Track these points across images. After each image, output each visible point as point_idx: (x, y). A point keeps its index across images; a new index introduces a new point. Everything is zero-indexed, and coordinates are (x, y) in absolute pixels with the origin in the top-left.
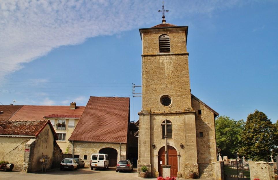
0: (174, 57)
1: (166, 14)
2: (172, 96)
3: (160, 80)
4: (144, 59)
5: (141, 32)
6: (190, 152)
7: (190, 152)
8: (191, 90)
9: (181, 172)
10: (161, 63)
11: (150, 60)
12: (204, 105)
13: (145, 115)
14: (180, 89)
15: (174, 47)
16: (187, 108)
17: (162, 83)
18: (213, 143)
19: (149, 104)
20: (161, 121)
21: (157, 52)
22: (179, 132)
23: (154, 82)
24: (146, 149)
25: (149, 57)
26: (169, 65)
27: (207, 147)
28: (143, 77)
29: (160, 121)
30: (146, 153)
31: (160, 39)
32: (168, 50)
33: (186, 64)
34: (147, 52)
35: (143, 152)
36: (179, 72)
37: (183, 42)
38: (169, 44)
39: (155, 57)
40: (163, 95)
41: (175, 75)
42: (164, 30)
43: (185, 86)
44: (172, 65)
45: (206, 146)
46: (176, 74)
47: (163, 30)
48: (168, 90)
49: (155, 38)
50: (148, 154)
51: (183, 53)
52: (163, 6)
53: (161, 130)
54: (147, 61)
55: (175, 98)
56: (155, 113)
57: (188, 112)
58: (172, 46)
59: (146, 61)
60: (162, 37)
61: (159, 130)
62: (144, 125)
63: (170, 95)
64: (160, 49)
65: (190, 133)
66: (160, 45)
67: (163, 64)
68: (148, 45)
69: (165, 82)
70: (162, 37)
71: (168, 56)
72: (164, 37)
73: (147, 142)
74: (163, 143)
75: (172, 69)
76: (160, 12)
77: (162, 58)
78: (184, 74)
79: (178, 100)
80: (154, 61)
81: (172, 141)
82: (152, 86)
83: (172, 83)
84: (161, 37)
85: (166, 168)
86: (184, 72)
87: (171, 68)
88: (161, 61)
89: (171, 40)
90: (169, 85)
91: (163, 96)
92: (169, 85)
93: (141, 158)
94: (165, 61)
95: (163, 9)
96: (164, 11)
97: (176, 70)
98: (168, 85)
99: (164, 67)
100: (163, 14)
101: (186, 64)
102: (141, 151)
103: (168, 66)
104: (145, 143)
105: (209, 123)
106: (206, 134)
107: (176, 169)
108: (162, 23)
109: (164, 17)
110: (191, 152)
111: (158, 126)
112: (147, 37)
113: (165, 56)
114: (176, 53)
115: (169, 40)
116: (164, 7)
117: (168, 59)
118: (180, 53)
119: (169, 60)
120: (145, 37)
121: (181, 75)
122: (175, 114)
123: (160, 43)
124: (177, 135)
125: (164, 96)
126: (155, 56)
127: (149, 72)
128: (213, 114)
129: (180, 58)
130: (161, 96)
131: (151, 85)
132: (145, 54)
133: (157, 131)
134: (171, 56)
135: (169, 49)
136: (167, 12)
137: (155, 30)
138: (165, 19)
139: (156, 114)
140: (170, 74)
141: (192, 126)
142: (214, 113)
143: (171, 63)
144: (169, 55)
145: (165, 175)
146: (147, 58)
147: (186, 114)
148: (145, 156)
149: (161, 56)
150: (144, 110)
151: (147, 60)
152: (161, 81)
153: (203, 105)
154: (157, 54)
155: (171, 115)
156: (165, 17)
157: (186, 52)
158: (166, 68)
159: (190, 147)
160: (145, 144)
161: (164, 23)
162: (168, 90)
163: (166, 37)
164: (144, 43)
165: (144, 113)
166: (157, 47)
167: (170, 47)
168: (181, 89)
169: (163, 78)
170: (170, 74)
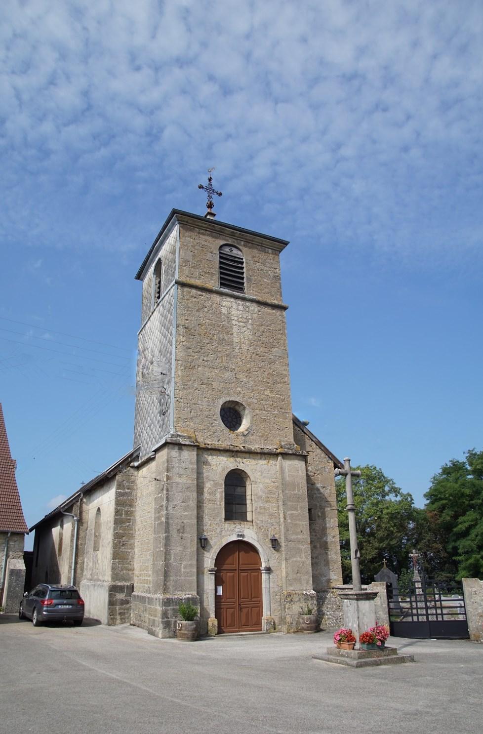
0: (254, 307)
1: (215, 199)
2: (249, 405)
4: (183, 292)
6: (295, 559)
7: (295, 559)
9: (272, 616)
10: (224, 314)
11: (195, 300)
12: (314, 439)
13: (183, 447)
14: (267, 392)
16: (284, 441)
17: (226, 369)
18: (334, 537)
19: (191, 418)
20: (223, 470)
21: (214, 283)
22: (267, 505)
24: (185, 549)
25: (194, 291)
27: (321, 547)
28: (177, 342)
29: (219, 469)
30: (184, 563)
31: (220, 253)
32: (239, 287)
33: (281, 332)
34: (187, 276)
35: (175, 560)
39: (209, 295)
40: (228, 399)
42: (235, 233)
43: (280, 385)
45: (318, 546)
46: (260, 350)
47: (232, 232)
48: (239, 389)
50: (191, 565)
51: (275, 302)
52: (210, 180)
53: (221, 496)
54: (187, 300)
55: (257, 412)
56: (209, 447)
57: (290, 452)
58: (249, 280)
60: (227, 250)
61: (218, 496)
62: (180, 476)
63: (244, 403)
65: (296, 509)
67: (229, 319)
68: (193, 259)
69: (234, 367)
70: (227, 250)
71: (240, 302)
72: (231, 251)
73: (188, 529)
74: (228, 533)
77: (227, 302)
79: (265, 420)
81: (251, 527)
83: (249, 371)
84: (223, 248)
85: (363, 602)
87: (248, 334)
88: (224, 310)
90: (242, 377)
91: (226, 402)
92: (242, 377)
93: (171, 578)
94: (234, 312)
96: (210, 190)
99: (232, 327)
101: (281, 332)
102: (171, 557)
104: (181, 531)
105: (324, 487)
106: (320, 514)
107: (233, 610)
109: (210, 206)
110: (299, 559)
111: (216, 484)
112: (190, 237)
113: (232, 300)
117: (241, 307)
118: (269, 301)
121: (270, 357)
122: (257, 453)
124: (262, 511)
125: (232, 401)
128: (333, 465)
129: (269, 314)
130: (221, 402)
132: (183, 279)
133: (213, 498)
134: (248, 304)
137: (214, 226)
138: (213, 211)
139: (211, 449)
140: (245, 347)
141: (299, 491)
142: (334, 463)
143: (248, 322)
145: (363, 623)
146: (190, 293)
147: (284, 456)
148: (183, 570)
149: (224, 297)
150: (179, 433)
151: (188, 297)
152: (222, 362)
153: (312, 440)
155: (247, 455)
158: (235, 330)
159: (297, 545)
160: (183, 533)
162: (239, 389)
163: (235, 252)
164: (181, 252)
165: (183, 443)
166: (212, 271)
168: (271, 392)
169: (228, 355)
170: (245, 347)
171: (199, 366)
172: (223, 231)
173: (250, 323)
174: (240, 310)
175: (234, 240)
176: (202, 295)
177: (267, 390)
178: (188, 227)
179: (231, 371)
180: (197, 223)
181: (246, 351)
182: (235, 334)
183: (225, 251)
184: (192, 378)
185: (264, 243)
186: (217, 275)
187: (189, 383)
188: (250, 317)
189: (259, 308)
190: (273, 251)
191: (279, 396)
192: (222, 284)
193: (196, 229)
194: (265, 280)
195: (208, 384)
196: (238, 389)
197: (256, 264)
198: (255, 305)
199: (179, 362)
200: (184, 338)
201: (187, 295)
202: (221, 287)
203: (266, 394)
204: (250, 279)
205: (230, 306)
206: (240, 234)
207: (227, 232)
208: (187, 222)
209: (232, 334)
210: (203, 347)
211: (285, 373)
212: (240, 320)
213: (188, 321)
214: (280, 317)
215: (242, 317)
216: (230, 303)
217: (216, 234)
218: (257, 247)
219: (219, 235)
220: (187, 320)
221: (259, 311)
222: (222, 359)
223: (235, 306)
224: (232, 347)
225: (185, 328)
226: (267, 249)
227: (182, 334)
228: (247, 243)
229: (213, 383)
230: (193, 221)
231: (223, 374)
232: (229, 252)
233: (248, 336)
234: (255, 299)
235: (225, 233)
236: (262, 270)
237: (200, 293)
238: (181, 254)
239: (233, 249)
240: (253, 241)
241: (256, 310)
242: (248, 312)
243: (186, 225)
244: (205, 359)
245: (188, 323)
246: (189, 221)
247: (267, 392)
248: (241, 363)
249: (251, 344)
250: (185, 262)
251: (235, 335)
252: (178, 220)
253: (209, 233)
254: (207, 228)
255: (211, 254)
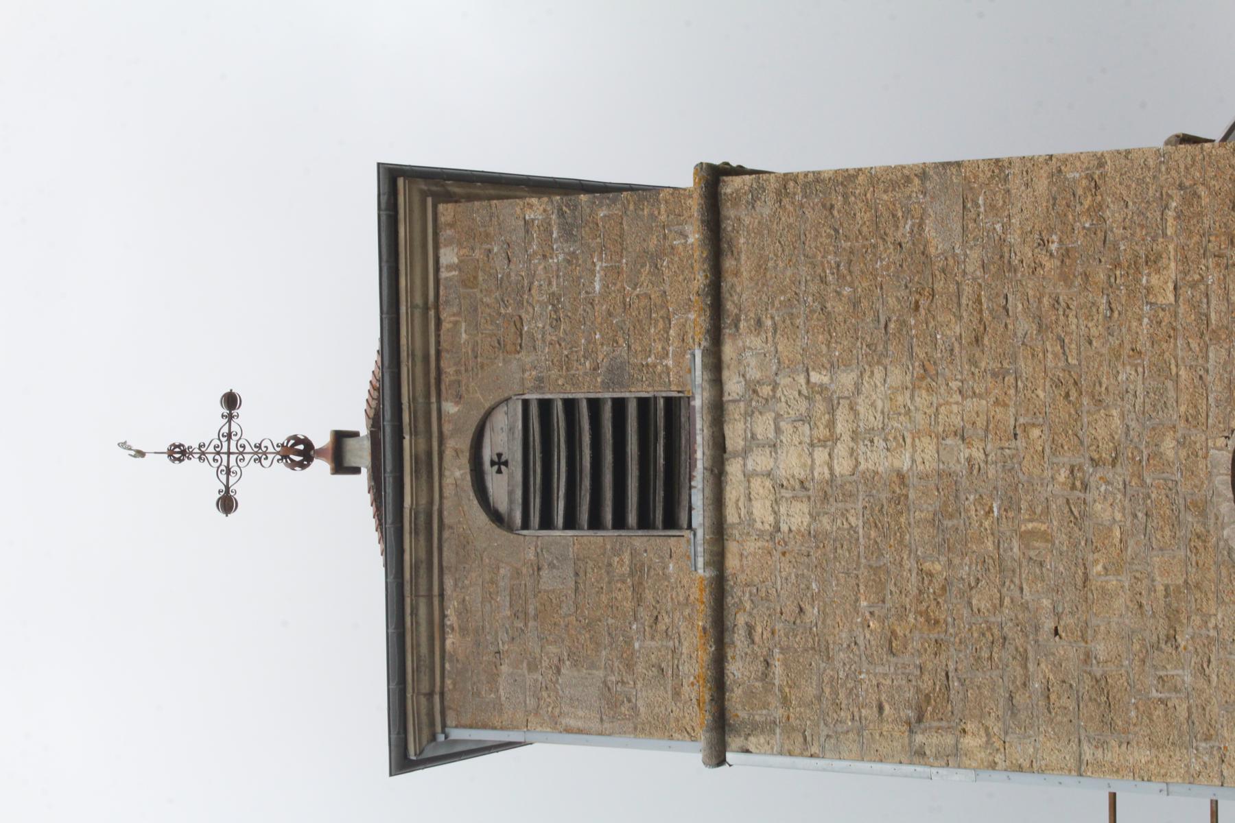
3: (1027, 536)
4: (755, 728)
5: (429, 753)
8: (1186, 139)
10: (814, 517)
11: (778, 669)
14: (1162, 283)
15: (622, 351)
17: (1077, 517)
23: (1059, 616)
25: (736, 669)
26: (842, 414)
31: (526, 525)
33: (838, 202)
34: (677, 694)
36: (939, 286)
37: (568, 233)
38: (594, 404)
39: (737, 595)
41: (977, 340)
42: (416, 459)
43: (1114, 214)
44: (847, 379)
46: (955, 329)
47: (416, 472)
48: (1168, 446)
49: (517, 573)
51: (694, 235)
52: (178, 453)
54: (785, 702)
58: (616, 374)
59: (780, 713)
60: (502, 488)
64: (645, 523)
66: (596, 523)
68: (593, 666)
69: (1063, 475)
71: (735, 435)
72: (500, 463)
75: (897, 376)
76: (241, 493)
78: (957, 227)
80: (791, 608)
82: (1100, 649)
84: (502, 506)
86: (930, 231)
88: (797, 516)
89: (540, 383)
94: (791, 463)
95: (202, 456)
97: (903, 323)
98: (1102, 433)
99: (870, 479)
100: (260, 453)
101: (838, 202)
103: (855, 435)
108: (362, 481)
112: (493, 678)
113: (734, 469)
114: (696, 320)
115: (545, 405)
116: (191, 442)
117: (763, 426)
118: (700, 280)
119: (778, 417)
120: (498, 707)
123: (571, 523)
126: (719, 586)
127: (926, 684)
129: (761, 267)
131: (1088, 657)
132: (699, 718)
134: (733, 386)
135: (644, 404)
136: (240, 411)
137: (416, 568)
138: (321, 440)
143: (823, 388)
144: (718, 410)
149: (731, 516)
151: (774, 701)
152: (1046, 537)
154: (703, 572)
156: (298, 441)
157: (695, 206)
158: (877, 460)
161: (360, 453)
162: (1168, 446)
164: (572, 723)
166: (622, 564)
167: (632, 394)
168: (1153, 261)
169: (1011, 505)
170: (955, 412)
171: (1088, 655)
172: (422, 518)
173: (826, 380)
174: (778, 430)
175: (449, 453)
176: (750, 629)
177: (1149, 290)
178: (448, 682)
179: (1085, 487)
180: (424, 650)
181: (968, 403)
182: (897, 464)
183: (511, 501)
184: (1154, 694)
185: (419, 300)
186: (637, 543)
187: (1182, 713)
188: (801, 379)
189: (742, 325)
190: (442, 239)
191: (1170, 214)
192: (671, 522)
193: (448, 643)
194: (597, 287)
195: (1173, 616)
196: (1170, 454)
197: (533, 339)
198: (728, 351)
199: (1088, 756)
200: (969, 727)
201: (766, 705)
202: (690, 527)
203: (1172, 299)
204: (610, 370)
205: (768, 483)
206: (414, 432)
207: (423, 501)
208: (430, 695)
209: (901, 477)
210: (996, 631)
211: (1042, 185)
212: (822, 432)
213: (887, 707)
214: (766, 209)
215: (806, 419)
216: (756, 483)
217: (445, 549)
218: (446, 326)
219: (446, 534)
220: (881, 708)
221: (759, 323)
222: (1031, 533)
223: (760, 461)
224: (965, 482)
225: (920, 720)
226: (444, 274)
227: (949, 740)
228: (446, 380)
229: (1160, 588)
230: (416, 670)
231: (1110, 529)
232: (511, 476)
233: (895, 390)
234: (705, 352)
235: (431, 502)
236: (554, 300)
237: (739, 639)
238: (580, 724)
239: (487, 455)
240: (426, 357)
241: (755, 342)
242: (775, 386)
243: (442, 694)
244: (1049, 625)
245: (893, 705)
246: (425, 687)
247: (1162, 283)
248: (1035, 432)
249: (927, 375)
250: (613, 705)
251: (903, 462)
252: (433, 738)
253: (449, 583)
254: (430, 597)
255: (544, 573)
